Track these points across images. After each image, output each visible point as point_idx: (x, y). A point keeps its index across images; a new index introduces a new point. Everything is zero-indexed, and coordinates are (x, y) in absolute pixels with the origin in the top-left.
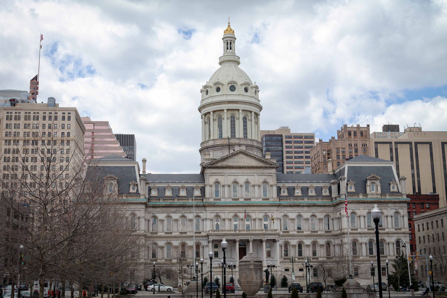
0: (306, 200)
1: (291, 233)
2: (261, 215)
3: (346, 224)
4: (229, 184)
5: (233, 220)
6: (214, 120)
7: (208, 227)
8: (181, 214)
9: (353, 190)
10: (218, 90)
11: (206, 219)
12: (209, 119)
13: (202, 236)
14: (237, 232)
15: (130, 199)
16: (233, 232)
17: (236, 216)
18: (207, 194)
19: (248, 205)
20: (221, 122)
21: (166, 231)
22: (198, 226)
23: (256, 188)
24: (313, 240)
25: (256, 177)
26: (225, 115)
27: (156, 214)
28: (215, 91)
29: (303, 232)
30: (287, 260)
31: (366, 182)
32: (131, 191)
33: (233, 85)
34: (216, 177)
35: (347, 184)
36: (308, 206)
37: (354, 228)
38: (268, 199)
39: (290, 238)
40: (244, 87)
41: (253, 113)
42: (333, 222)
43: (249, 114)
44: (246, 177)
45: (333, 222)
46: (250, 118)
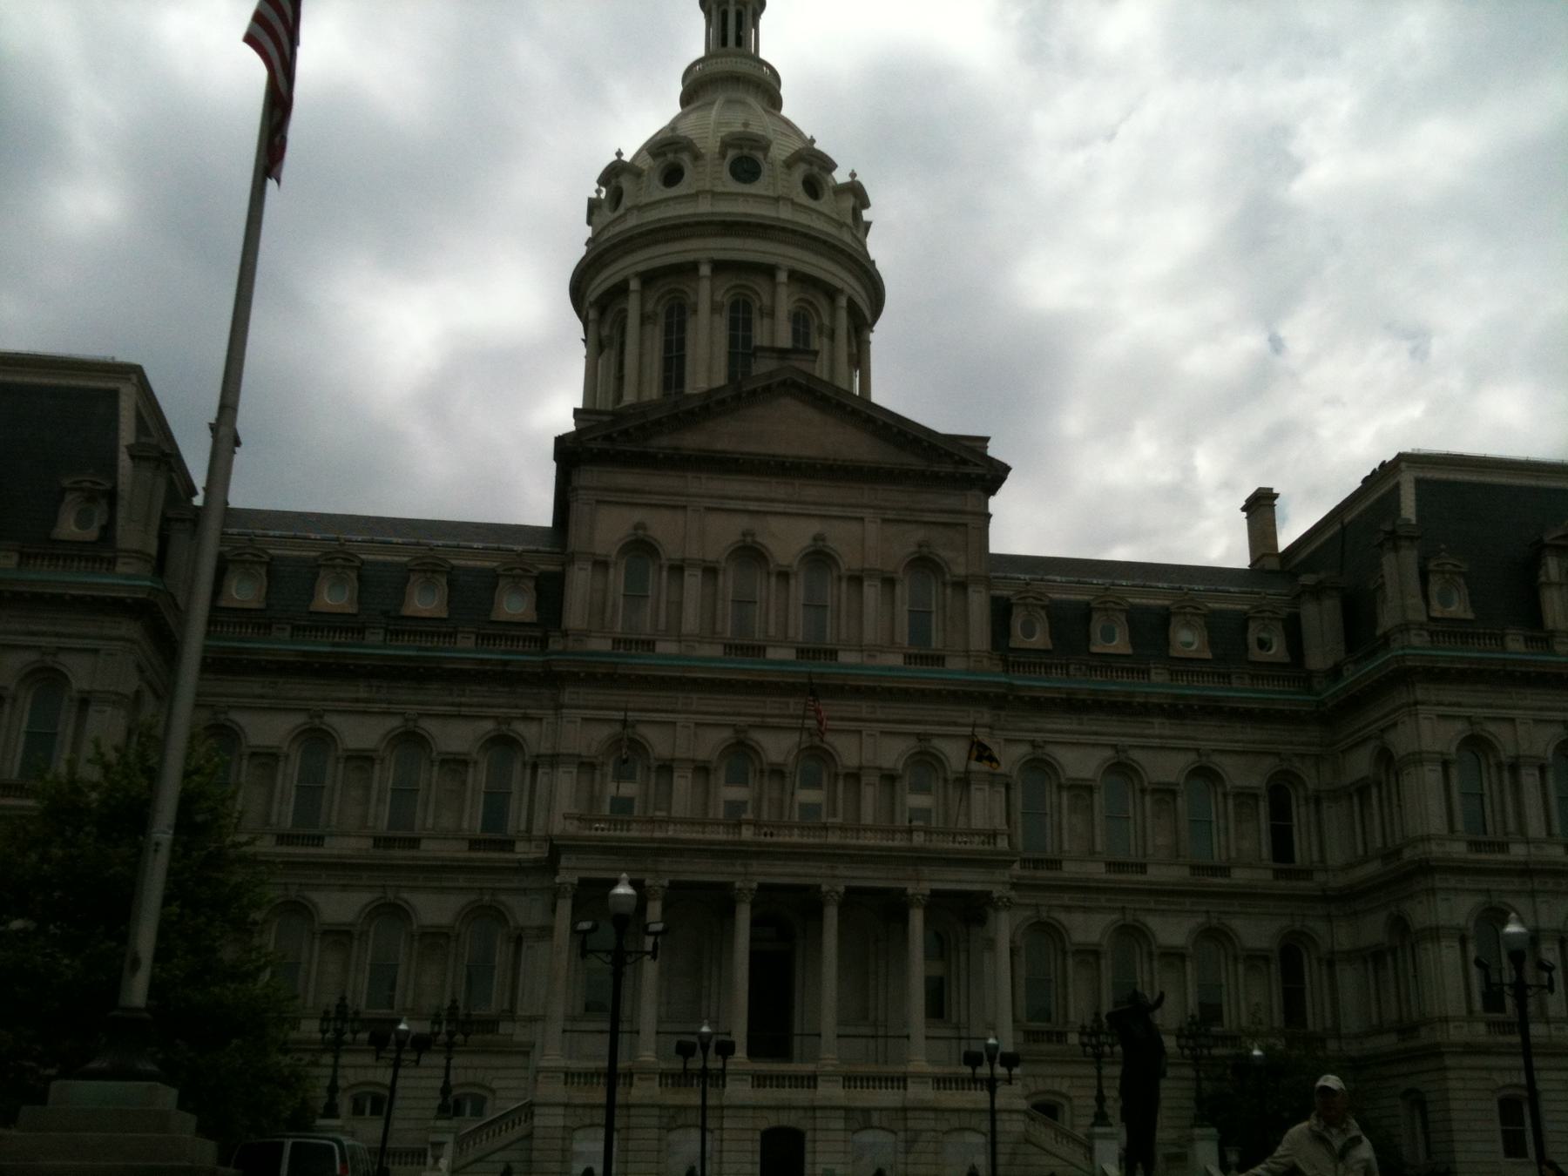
0: (1158, 676)
1: (1070, 869)
2: (892, 753)
3: (1428, 809)
4: (711, 557)
5: (722, 774)
6: (645, 319)
7: (557, 805)
8: (395, 722)
9: (1458, 608)
10: (672, 176)
11: (554, 760)
12: (622, 316)
13: (520, 869)
14: (747, 834)
15: (46, 576)
16: (720, 835)
17: (741, 752)
18: (575, 615)
20: (682, 328)
21: (288, 824)
22: (496, 805)
23: (872, 592)
24: (1201, 919)
26: (705, 288)
27: (236, 717)
28: (656, 182)
29: (1143, 868)
30: (1045, 1047)
31: (1533, 564)
32: (68, 527)
33: (746, 151)
35: (1424, 576)
36: (1177, 711)
37: (1482, 838)
38: (939, 660)
39: (1066, 899)
40: (800, 171)
41: (843, 302)
42: (1318, 811)
43: (823, 304)
44: (815, 527)
45: (1318, 811)
46: (826, 321)
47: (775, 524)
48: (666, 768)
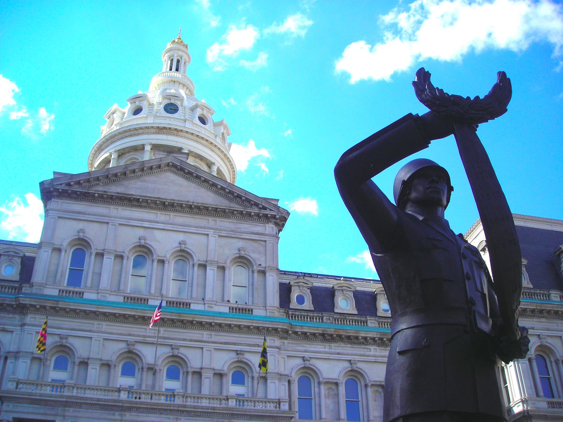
18: (38, 276)
19: (178, 317)
25: (213, 239)
34: (81, 225)
44: (181, 237)
47: (157, 233)
48: (84, 363)
